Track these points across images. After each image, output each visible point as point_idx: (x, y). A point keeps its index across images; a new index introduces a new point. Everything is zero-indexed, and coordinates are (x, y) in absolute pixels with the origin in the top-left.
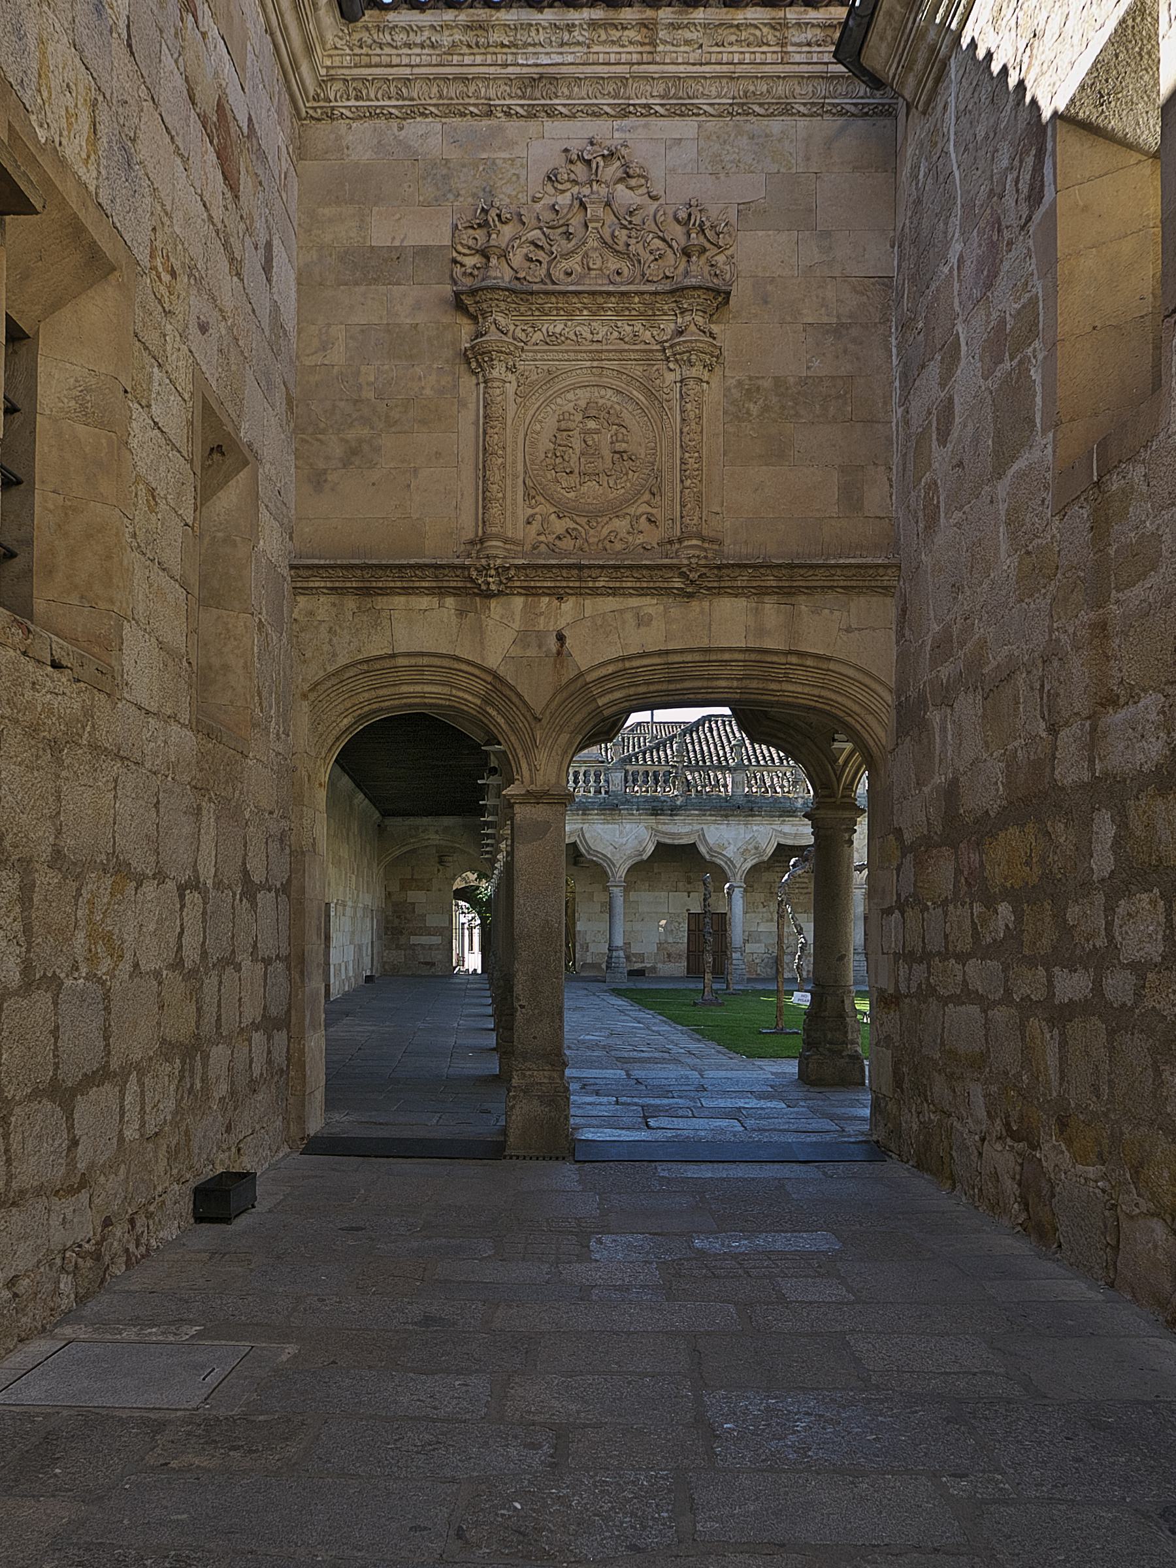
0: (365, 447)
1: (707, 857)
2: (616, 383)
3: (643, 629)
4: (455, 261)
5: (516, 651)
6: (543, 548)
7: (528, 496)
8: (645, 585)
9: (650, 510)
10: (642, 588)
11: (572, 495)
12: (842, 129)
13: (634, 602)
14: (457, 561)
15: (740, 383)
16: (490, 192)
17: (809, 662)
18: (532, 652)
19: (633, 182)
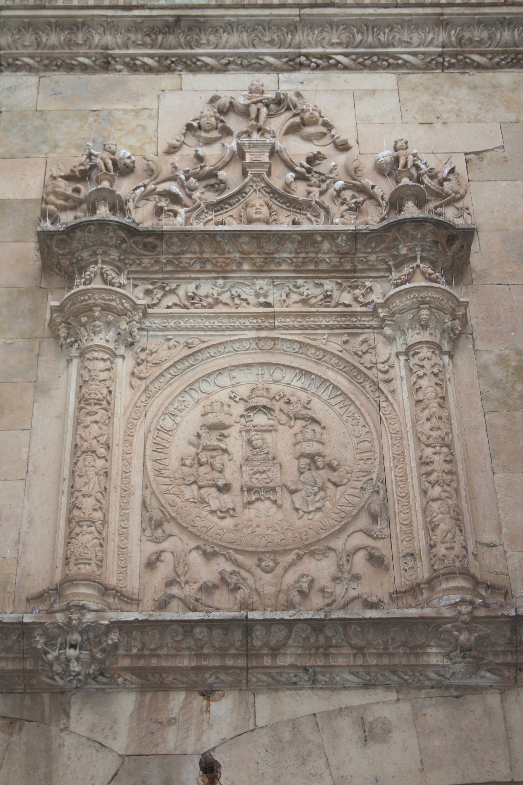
3: (375, 749)
9: (369, 542)
11: (229, 522)
13: (354, 699)
15: (503, 360)
19: (310, 130)
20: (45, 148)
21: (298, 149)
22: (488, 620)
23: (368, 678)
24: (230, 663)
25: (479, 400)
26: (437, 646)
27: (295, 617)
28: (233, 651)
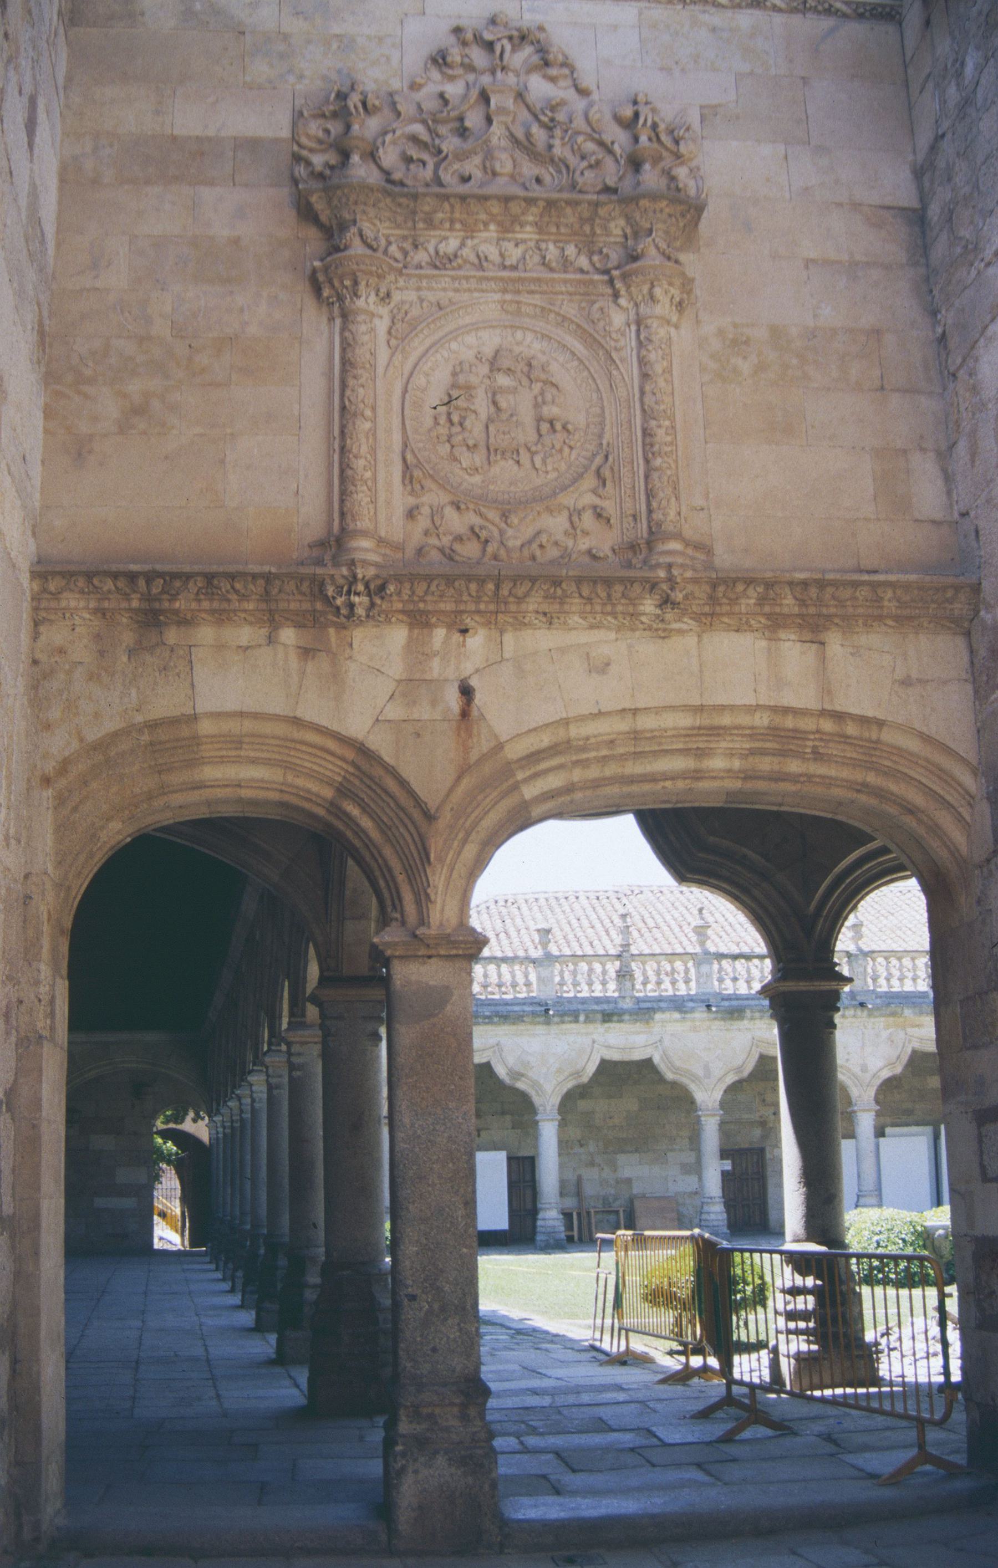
0: (156, 404)
1: (507, 1080)
4: (297, 158)
5: (394, 712)
6: (435, 555)
9: (598, 501)
11: (477, 479)
12: (833, 30)
15: (721, 332)
17: (851, 729)
18: (424, 712)
19: (553, 72)
20: (291, 79)
21: (539, 88)
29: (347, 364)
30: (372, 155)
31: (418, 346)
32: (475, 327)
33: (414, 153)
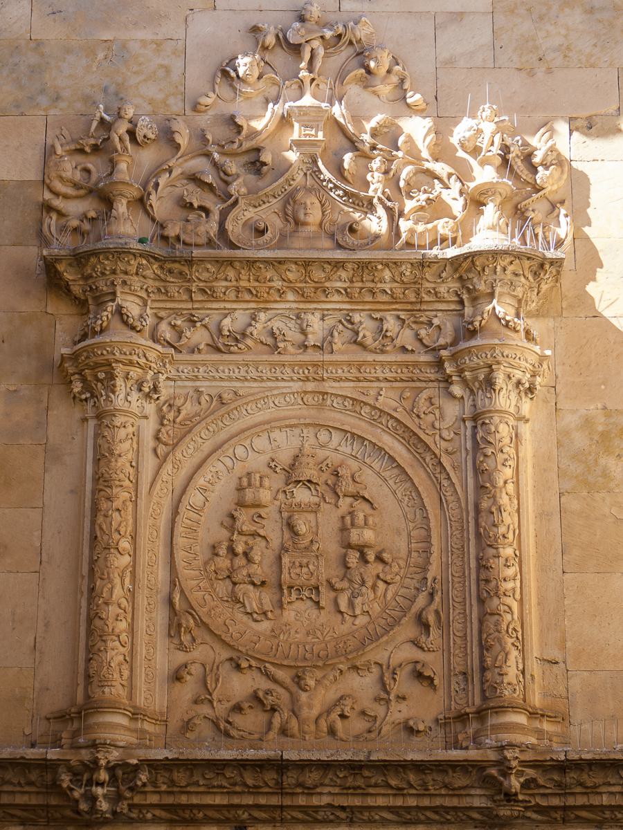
2: (351, 422)
4: (48, 208)
6: (206, 730)
7: (174, 628)
8: (412, 802)
9: (420, 655)
10: (408, 809)
11: (265, 626)
14: (32, 753)
15: (587, 423)
16: (117, 98)
22: (535, 765)
23: (409, 817)
24: (262, 801)
25: (555, 477)
26: (481, 788)
27: (333, 758)
28: (267, 790)
29: (102, 482)
30: (141, 202)
31: (188, 454)
32: (267, 426)
33: (197, 197)
